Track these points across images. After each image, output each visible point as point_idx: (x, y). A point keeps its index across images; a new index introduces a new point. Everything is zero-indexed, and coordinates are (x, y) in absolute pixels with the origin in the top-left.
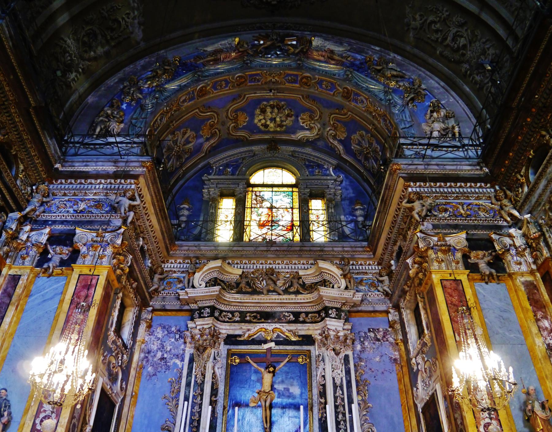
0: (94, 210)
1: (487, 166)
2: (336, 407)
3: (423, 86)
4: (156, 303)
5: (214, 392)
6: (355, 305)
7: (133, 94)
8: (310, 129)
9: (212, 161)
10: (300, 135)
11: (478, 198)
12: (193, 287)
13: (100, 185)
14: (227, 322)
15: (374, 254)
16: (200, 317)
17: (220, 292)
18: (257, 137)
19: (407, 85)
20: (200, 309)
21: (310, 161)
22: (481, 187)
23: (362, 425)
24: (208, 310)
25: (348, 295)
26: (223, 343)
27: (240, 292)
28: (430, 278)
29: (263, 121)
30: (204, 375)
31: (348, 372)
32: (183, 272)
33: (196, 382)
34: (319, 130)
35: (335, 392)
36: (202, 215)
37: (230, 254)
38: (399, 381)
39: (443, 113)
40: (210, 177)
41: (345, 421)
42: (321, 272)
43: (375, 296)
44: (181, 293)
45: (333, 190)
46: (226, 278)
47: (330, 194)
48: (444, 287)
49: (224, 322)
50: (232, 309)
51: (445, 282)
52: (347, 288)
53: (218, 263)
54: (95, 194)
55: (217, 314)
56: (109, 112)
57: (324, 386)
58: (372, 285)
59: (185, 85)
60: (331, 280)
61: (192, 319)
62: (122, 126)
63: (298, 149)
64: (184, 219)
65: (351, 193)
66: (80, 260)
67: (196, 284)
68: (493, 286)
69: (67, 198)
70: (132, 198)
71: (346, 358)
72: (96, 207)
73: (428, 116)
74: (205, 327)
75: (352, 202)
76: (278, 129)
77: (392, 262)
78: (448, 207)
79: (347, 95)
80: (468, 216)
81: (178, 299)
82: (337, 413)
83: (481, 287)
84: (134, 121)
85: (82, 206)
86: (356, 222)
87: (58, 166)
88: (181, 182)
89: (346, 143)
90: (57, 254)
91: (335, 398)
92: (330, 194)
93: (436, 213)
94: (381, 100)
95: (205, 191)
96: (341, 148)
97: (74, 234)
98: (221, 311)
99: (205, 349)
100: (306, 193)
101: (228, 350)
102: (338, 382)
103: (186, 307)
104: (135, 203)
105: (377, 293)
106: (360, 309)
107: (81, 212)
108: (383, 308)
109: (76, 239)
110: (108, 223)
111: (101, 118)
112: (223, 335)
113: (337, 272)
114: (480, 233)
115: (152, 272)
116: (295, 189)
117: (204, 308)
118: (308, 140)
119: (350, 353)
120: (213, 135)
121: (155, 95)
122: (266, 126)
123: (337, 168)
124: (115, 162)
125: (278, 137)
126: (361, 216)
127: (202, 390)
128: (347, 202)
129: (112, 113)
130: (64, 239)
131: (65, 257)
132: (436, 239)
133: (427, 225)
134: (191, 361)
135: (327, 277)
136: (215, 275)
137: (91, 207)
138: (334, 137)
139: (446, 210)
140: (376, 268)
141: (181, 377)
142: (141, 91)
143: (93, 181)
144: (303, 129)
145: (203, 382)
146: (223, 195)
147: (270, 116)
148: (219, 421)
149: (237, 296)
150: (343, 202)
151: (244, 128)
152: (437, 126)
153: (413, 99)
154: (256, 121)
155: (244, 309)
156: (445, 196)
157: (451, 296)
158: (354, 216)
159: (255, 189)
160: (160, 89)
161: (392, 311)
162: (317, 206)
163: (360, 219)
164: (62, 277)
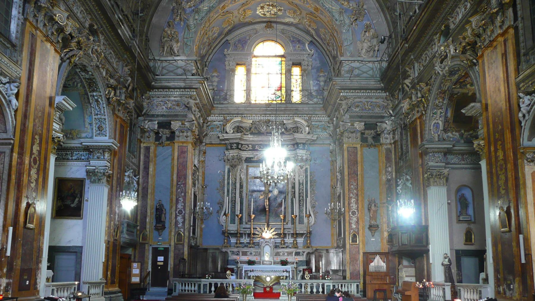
0: (177, 108)
1: (383, 83)
2: (299, 194)
3: (365, 7)
4: (206, 140)
5: (241, 187)
6: (314, 141)
7: (180, 15)
8: (294, 18)
9: (228, 38)
10: (287, 20)
11: (377, 98)
12: (226, 132)
13: (177, 93)
14: (245, 150)
15: (326, 112)
16: (231, 149)
17: (241, 136)
18: (259, 20)
19: (355, 6)
20: (231, 144)
21: (294, 37)
22: (379, 92)
23: (311, 201)
24: (235, 145)
25: (309, 137)
26: (244, 161)
27: (252, 134)
28: (343, 145)
29: (263, 13)
30: (236, 179)
31: (306, 177)
32: (219, 121)
33: (232, 182)
34: (300, 20)
35: (299, 187)
36: (226, 81)
37: (246, 112)
38: (332, 180)
39: (372, 32)
40: (229, 52)
41: (303, 200)
42: (296, 122)
43: (324, 134)
44: (220, 135)
45: (307, 63)
46: (243, 125)
47: (305, 66)
48: (348, 151)
49: (244, 150)
50: (248, 143)
51: (349, 149)
52: (309, 133)
53: (239, 119)
54: (175, 97)
55: (240, 147)
56: (169, 32)
57: (294, 183)
58: (324, 129)
59: (212, 6)
60: (302, 127)
61: (227, 149)
62: (179, 44)
63: (286, 27)
64: (215, 84)
65: (317, 64)
66: (176, 139)
67: (228, 131)
68: (372, 149)
69: (160, 99)
70: (195, 99)
71: (307, 169)
72: (178, 105)
73: (363, 35)
74: (234, 154)
75: (319, 70)
76: (273, 16)
77: (335, 119)
78: (360, 104)
79: (316, 9)
80: (369, 109)
81: (219, 137)
82: (299, 197)
83: (366, 150)
84: (185, 40)
85: (169, 105)
86: (320, 85)
87: (153, 83)
88: (211, 56)
89: (317, 31)
90: (165, 133)
91: (299, 189)
92: (305, 66)
93: (353, 108)
94: (336, 20)
95: (227, 63)
96: (313, 32)
97: (171, 124)
98: (242, 145)
99: (235, 166)
100: (291, 61)
101: (247, 166)
102: (301, 182)
103: (223, 142)
104: (197, 102)
105: (326, 133)
106: (316, 142)
107: (170, 108)
108: (328, 142)
109: (172, 127)
110: (185, 116)
111: (165, 39)
112: (244, 158)
113: (305, 123)
114: (373, 121)
115: (204, 122)
116: (283, 59)
117: (233, 143)
118: (292, 23)
119: (308, 167)
120: (229, 26)
121: (194, 17)
122: (264, 15)
123: (311, 43)
124: (184, 80)
125: (273, 20)
126: (322, 81)
127: (236, 186)
128: (315, 70)
129: (171, 33)
130: (165, 125)
131: (168, 136)
132: (350, 124)
133: (347, 116)
134: (229, 172)
135: (299, 125)
136: (237, 124)
137: (174, 105)
138: (310, 26)
139: (358, 106)
140: (326, 119)
141: (224, 179)
142: (184, 10)
143: (173, 90)
144: (289, 17)
145: (236, 182)
146: (238, 64)
147: (267, 10)
148: (244, 200)
149: (249, 136)
150: (312, 71)
151: (250, 16)
152: (366, 45)
153: (356, 20)
154: (258, 13)
155: (254, 143)
156: (360, 97)
157: (351, 155)
158: (318, 81)
159: (258, 59)
160: (197, 11)
161: (332, 144)
162: (296, 71)
163: (322, 83)
164: (169, 147)
